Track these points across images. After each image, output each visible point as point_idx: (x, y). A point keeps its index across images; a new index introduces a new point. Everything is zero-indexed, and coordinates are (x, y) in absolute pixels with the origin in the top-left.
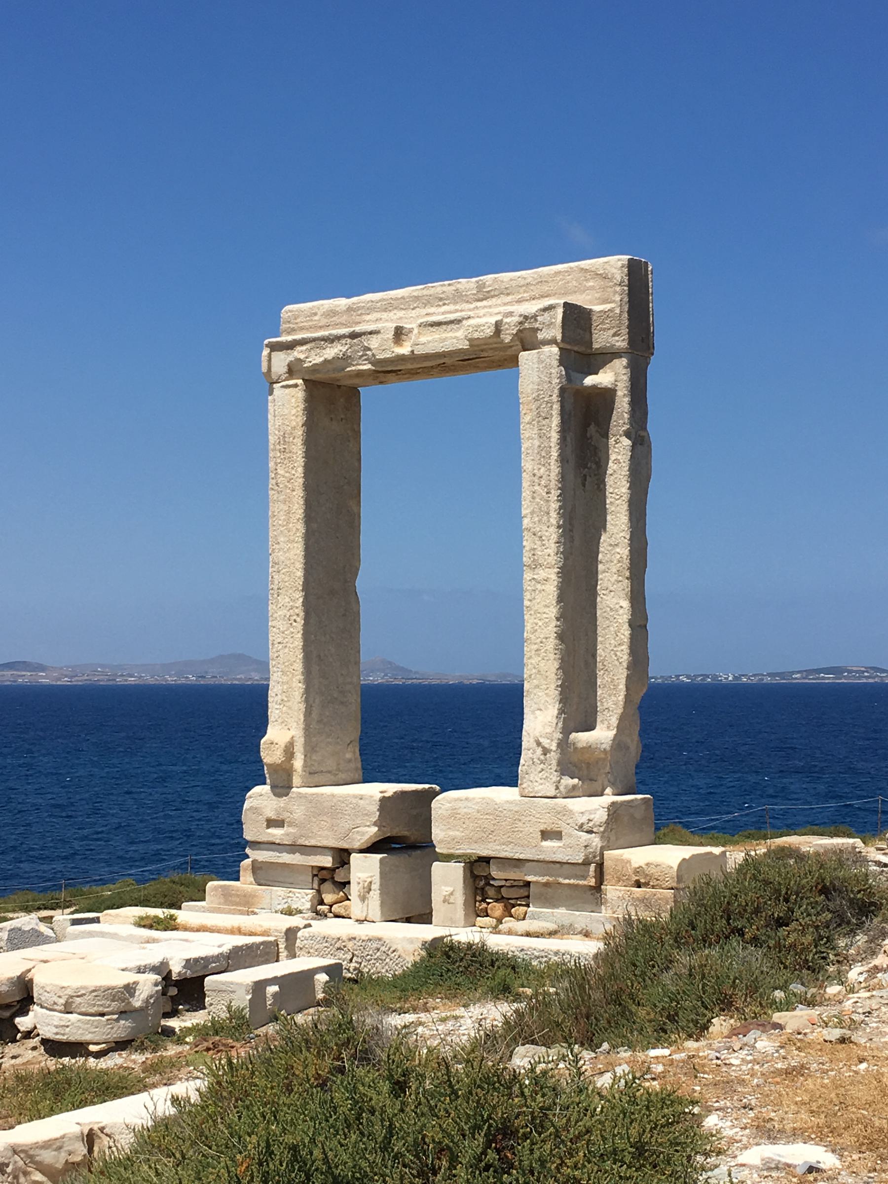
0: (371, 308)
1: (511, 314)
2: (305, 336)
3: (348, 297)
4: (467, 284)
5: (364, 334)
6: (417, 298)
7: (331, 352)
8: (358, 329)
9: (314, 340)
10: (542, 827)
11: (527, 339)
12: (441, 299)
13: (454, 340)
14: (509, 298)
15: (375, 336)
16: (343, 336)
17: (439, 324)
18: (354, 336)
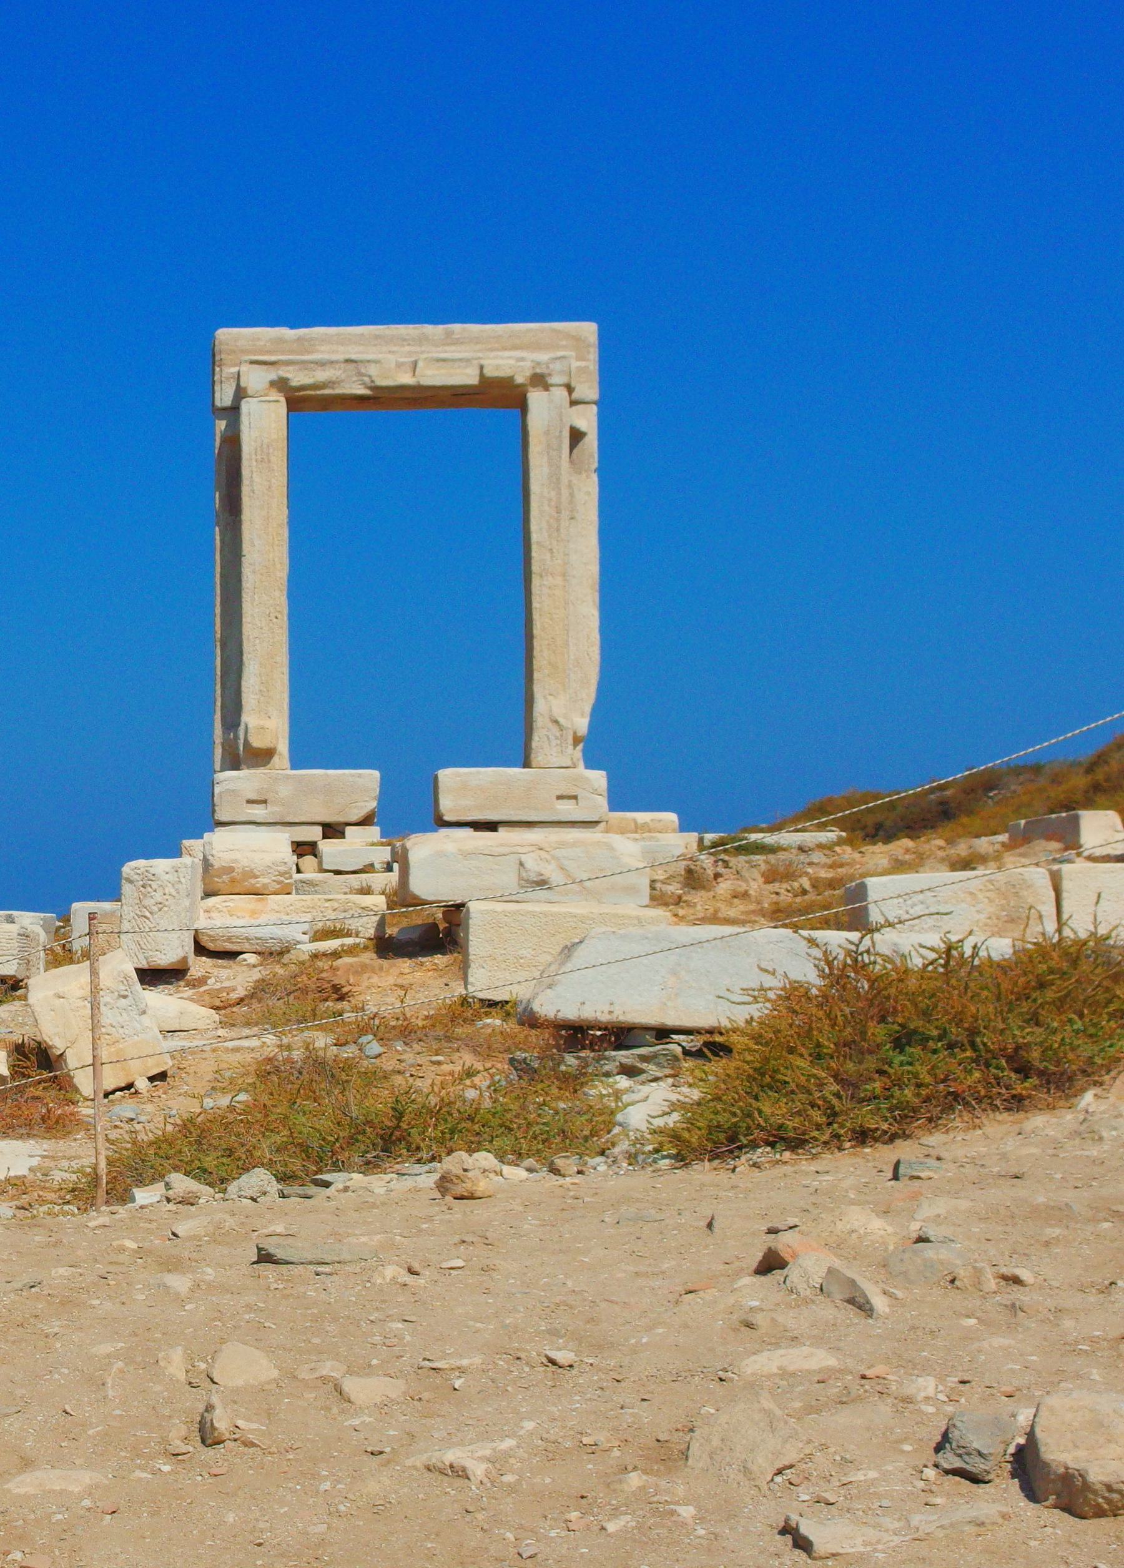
0: (324, 340)
1: (522, 359)
2: (291, 357)
3: (292, 326)
4: (429, 329)
5: (361, 361)
6: (377, 337)
7: (321, 376)
8: (353, 357)
9: (303, 362)
10: (559, 793)
11: (540, 380)
12: (405, 340)
13: (468, 377)
14: (478, 347)
15: (373, 365)
16: (337, 362)
17: (444, 360)
18: (347, 361)
